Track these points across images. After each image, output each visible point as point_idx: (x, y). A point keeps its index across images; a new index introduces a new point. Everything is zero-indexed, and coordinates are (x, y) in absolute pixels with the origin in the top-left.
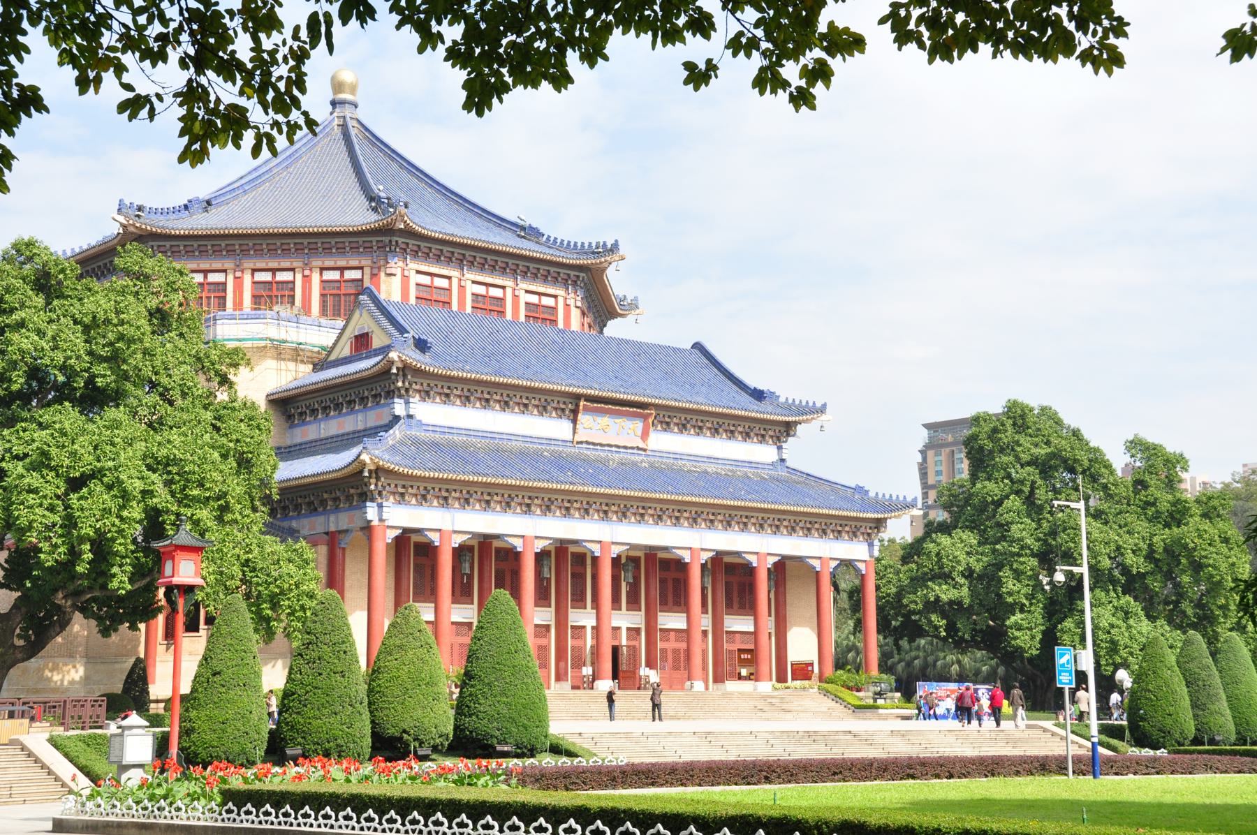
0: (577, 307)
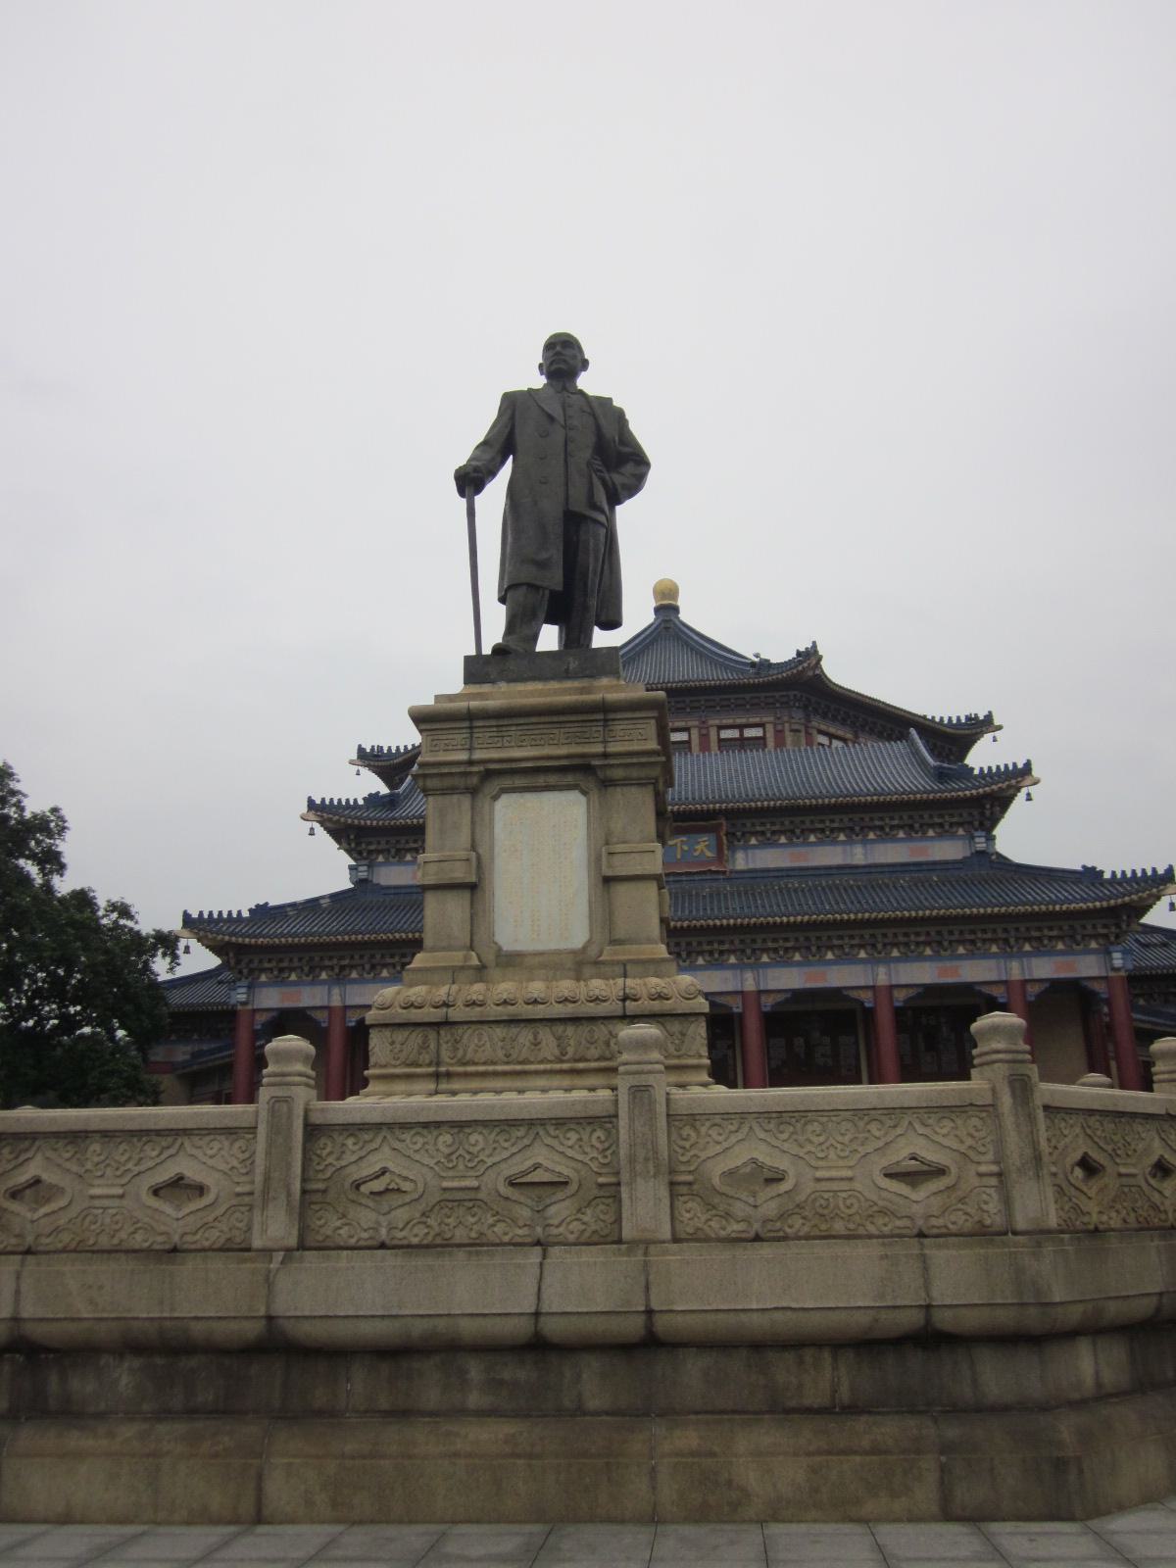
0: (792, 731)
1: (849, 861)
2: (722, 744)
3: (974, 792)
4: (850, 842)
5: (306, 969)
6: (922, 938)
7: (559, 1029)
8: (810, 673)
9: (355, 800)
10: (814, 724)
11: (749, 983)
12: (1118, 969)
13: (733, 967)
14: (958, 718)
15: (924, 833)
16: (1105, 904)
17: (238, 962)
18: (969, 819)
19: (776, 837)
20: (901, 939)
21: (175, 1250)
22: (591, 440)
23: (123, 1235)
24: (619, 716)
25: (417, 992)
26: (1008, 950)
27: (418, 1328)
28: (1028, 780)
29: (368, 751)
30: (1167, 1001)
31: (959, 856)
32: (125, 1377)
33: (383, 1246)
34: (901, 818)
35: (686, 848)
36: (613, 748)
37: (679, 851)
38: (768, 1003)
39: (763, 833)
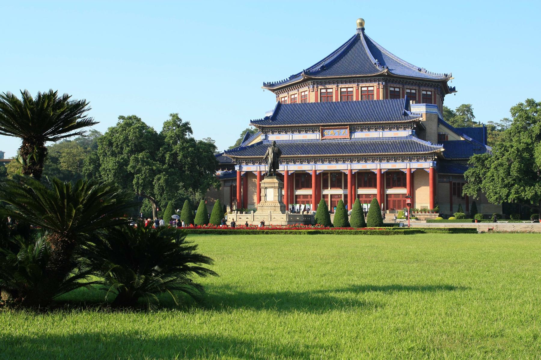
29: (266, 84)
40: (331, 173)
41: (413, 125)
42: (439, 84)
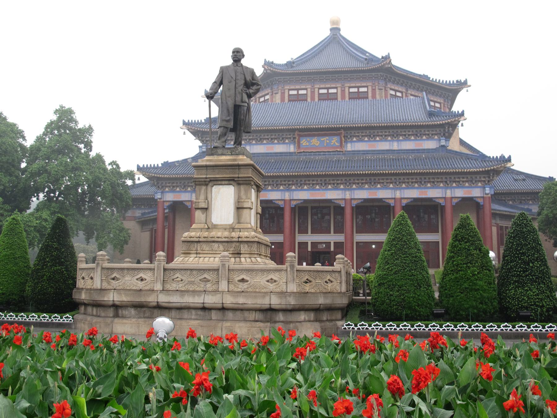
1: (391, 148)
2: (351, 94)
3: (441, 122)
4: (392, 140)
5: (183, 186)
6: (414, 180)
7: (224, 244)
8: (387, 66)
9: (201, 120)
10: (389, 86)
11: (348, 196)
12: (488, 194)
13: (342, 189)
14: (453, 81)
15: (422, 137)
16: (484, 169)
17: (158, 183)
18: (439, 132)
19: (364, 138)
20: (406, 180)
21: (141, 290)
22: (243, 82)
23: (131, 287)
24: (242, 167)
25: (193, 234)
26: (447, 185)
27: (183, 305)
28: (462, 118)
30: (521, 203)
31: (434, 147)
32: (133, 311)
33: (177, 290)
34: (413, 131)
35: (328, 141)
36: (239, 176)
37: (325, 142)
38: (354, 203)
39: (358, 136)
40: (312, 208)
41: (447, 130)
42: (450, 94)
